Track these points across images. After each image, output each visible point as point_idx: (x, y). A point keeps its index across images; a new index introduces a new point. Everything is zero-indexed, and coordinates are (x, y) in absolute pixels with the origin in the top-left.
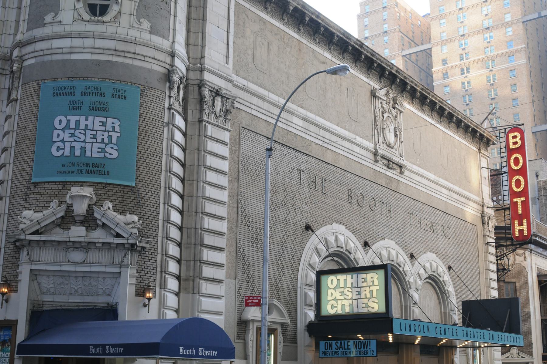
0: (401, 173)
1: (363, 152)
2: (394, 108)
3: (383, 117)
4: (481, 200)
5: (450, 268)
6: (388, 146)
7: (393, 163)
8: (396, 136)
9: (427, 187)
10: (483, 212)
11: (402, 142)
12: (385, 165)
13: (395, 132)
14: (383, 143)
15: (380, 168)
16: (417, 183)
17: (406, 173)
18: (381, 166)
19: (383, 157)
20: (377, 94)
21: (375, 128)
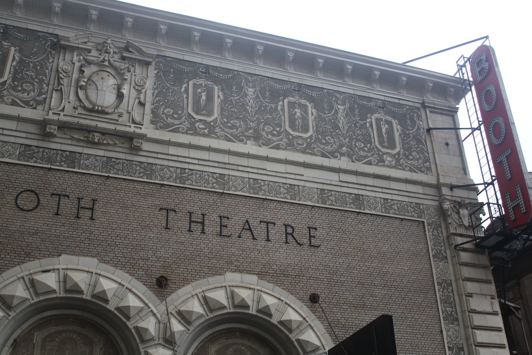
0: (136, 150)
1: (12, 125)
2: (123, 58)
3: (82, 72)
4: (435, 179)
5: (314, 299)
6: (92, 110)
7: (103, 134)
8: (120, 96)
9: (227, 166)
10: (441, 195)
11: (142, 104)
12: (79, 140)
13: (119, 88)
14: (75, 108)
15: (62, 144)
16: (196, 162)
17: (146, 146)
18: (69, 142)
19: (63, 127)
20: (62, 42)
21: (54, 89)
